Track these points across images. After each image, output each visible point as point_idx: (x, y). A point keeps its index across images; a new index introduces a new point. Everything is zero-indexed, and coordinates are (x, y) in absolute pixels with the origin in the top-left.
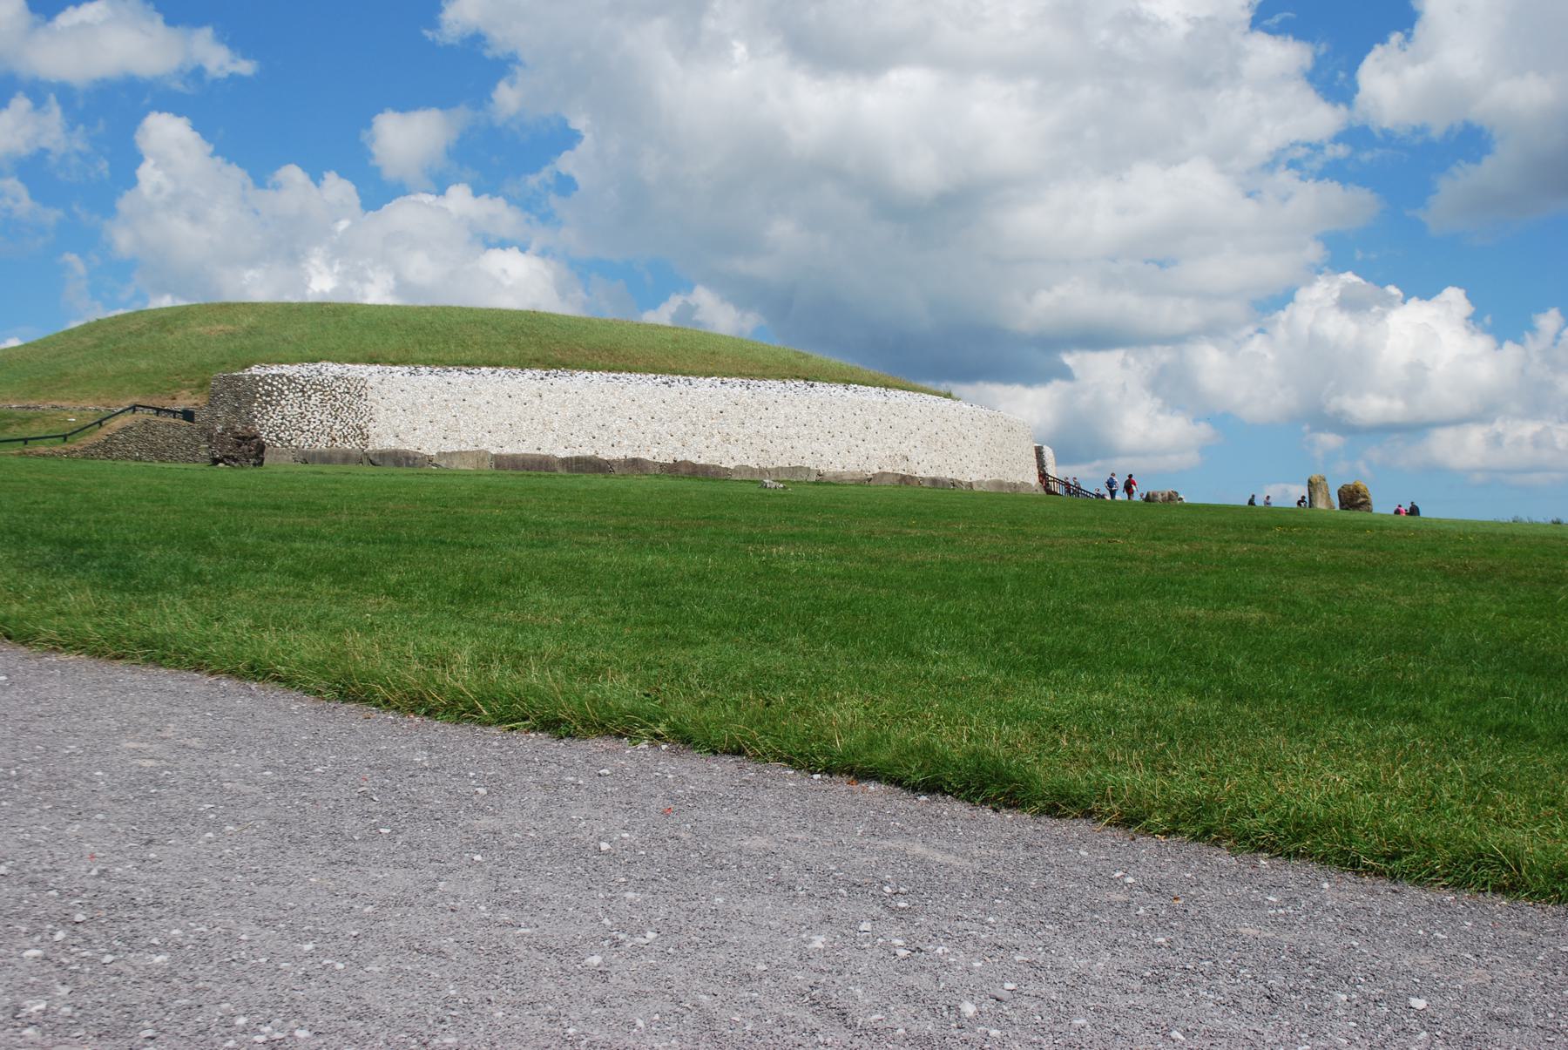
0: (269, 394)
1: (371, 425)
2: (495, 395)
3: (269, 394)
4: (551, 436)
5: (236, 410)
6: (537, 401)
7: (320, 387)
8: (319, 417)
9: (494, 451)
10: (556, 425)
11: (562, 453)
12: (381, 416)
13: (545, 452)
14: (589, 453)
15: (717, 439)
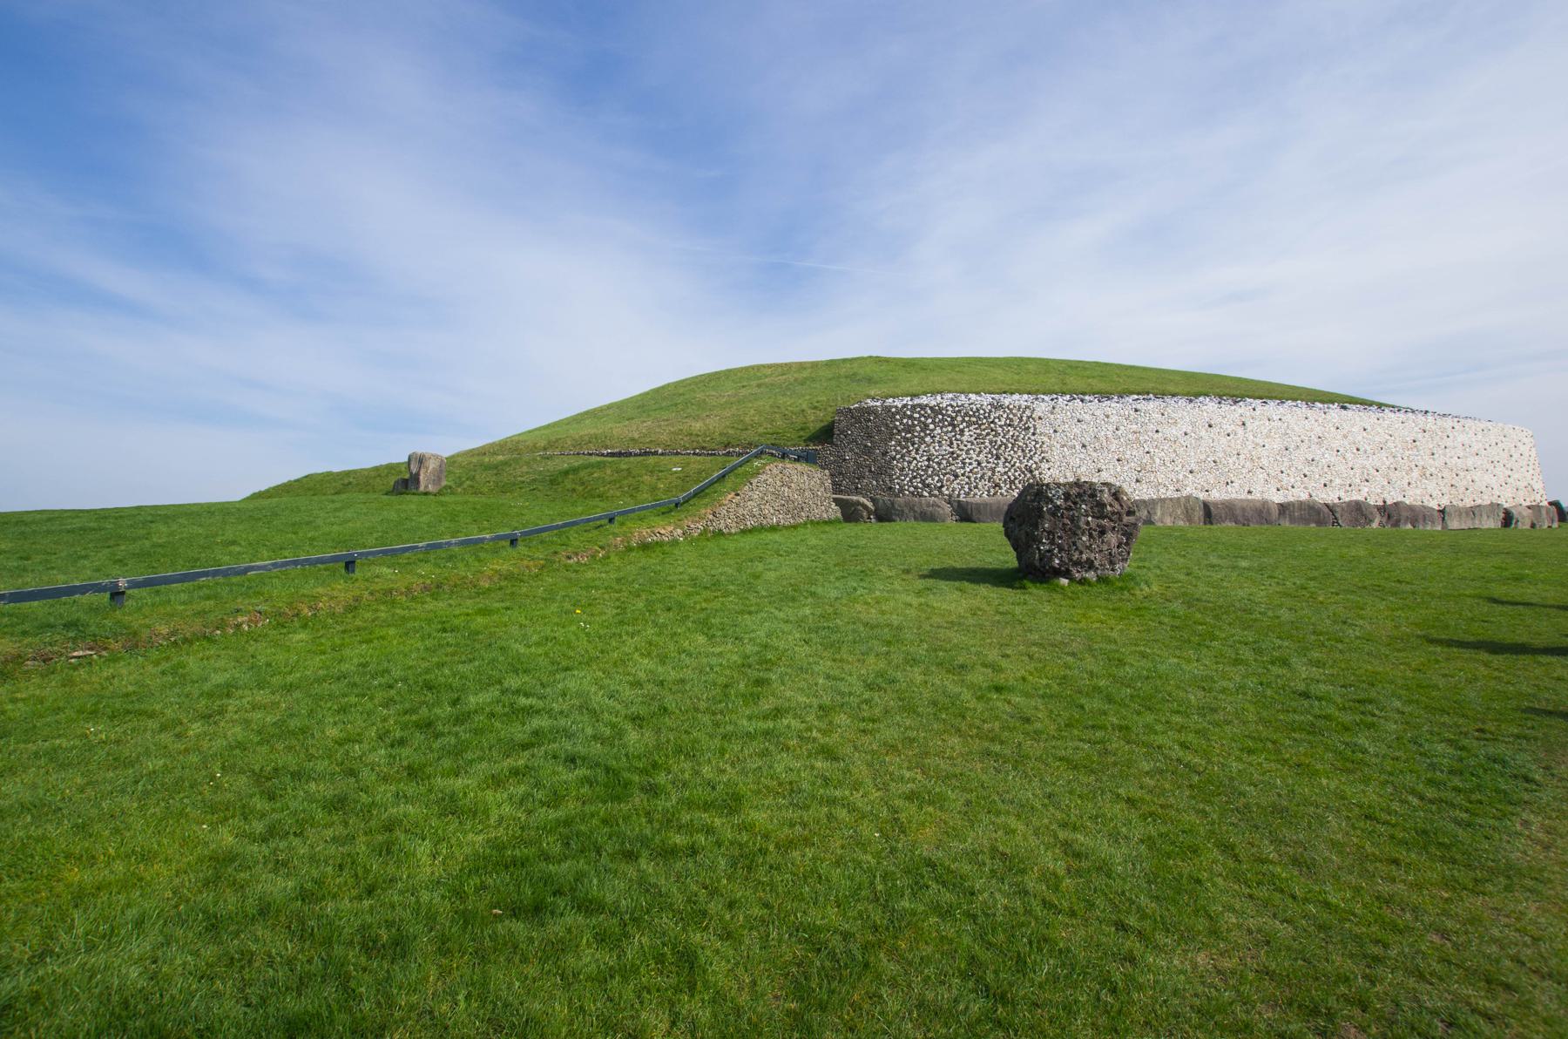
0: (909, 429)
1: (1044, 465)
2: (1193, 424)
3: (909, 429)
4: (1262, 476)
5: (868, 451)
6: (1240, 431)
7: (974, 418)
8: (974, 456)
9: (1202, 496)
10: (1265, 462)
11: (1278, 498)
12: (1055, 454)
13: (1257, 496)
14: (1304, 497)
15: (1416, 474)
